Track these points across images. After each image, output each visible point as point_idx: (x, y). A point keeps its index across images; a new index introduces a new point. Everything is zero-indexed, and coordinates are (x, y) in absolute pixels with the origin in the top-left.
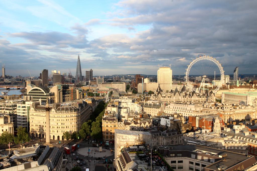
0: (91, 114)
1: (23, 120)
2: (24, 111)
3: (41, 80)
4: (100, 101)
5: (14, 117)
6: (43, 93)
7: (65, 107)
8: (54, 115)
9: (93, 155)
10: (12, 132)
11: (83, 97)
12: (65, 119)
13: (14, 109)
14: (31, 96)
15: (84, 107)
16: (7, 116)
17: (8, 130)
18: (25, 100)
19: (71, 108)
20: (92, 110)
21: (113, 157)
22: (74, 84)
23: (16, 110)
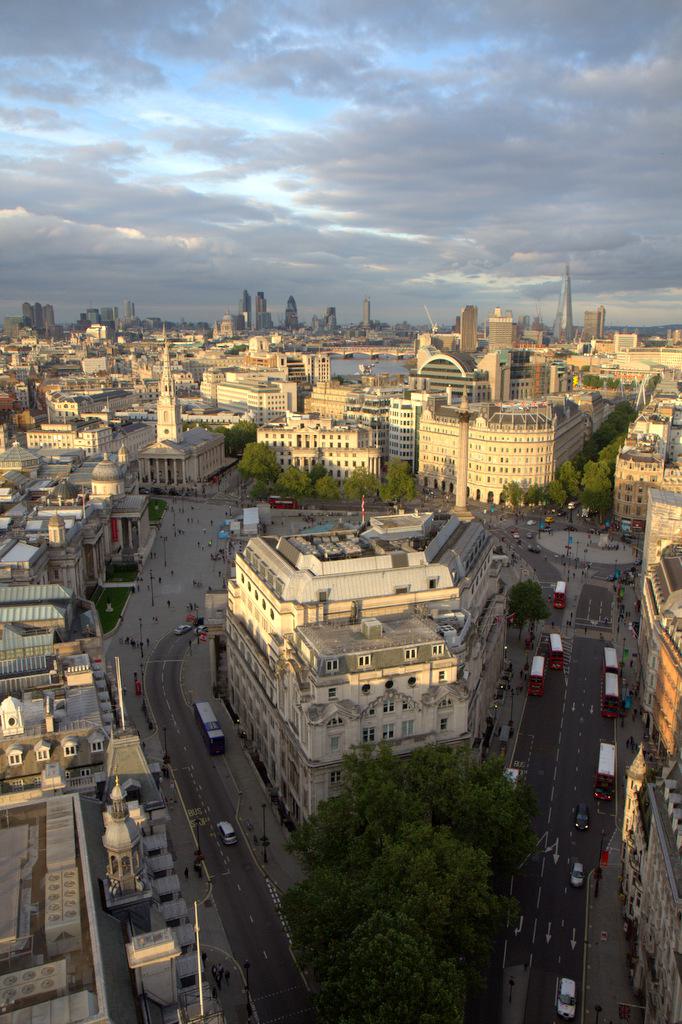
0: (586, 439)
1: (403, 442)
2: (407, 419)
3: (457, 335)
4: (618, 401)
5: (382, 430)
6: (459, 371)
7: (513, 414)
8: (483, 434)
9: (577, 552)
10: (373, 469)
11: (569, 389)
12: (511, 448)
13: (384, 411)
14: (428, 379)
15: (568, 416)
16: (364, 427)
17: (366, 465)
18: (410, 387)
19: (528, 417)
20: (591, 428)
21: (637, 567)
22: (546, 350)
23: (387, 415)
